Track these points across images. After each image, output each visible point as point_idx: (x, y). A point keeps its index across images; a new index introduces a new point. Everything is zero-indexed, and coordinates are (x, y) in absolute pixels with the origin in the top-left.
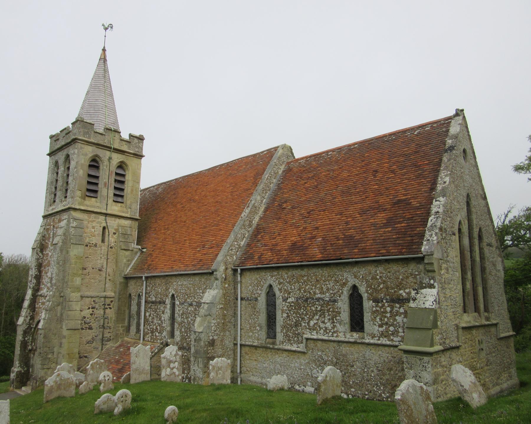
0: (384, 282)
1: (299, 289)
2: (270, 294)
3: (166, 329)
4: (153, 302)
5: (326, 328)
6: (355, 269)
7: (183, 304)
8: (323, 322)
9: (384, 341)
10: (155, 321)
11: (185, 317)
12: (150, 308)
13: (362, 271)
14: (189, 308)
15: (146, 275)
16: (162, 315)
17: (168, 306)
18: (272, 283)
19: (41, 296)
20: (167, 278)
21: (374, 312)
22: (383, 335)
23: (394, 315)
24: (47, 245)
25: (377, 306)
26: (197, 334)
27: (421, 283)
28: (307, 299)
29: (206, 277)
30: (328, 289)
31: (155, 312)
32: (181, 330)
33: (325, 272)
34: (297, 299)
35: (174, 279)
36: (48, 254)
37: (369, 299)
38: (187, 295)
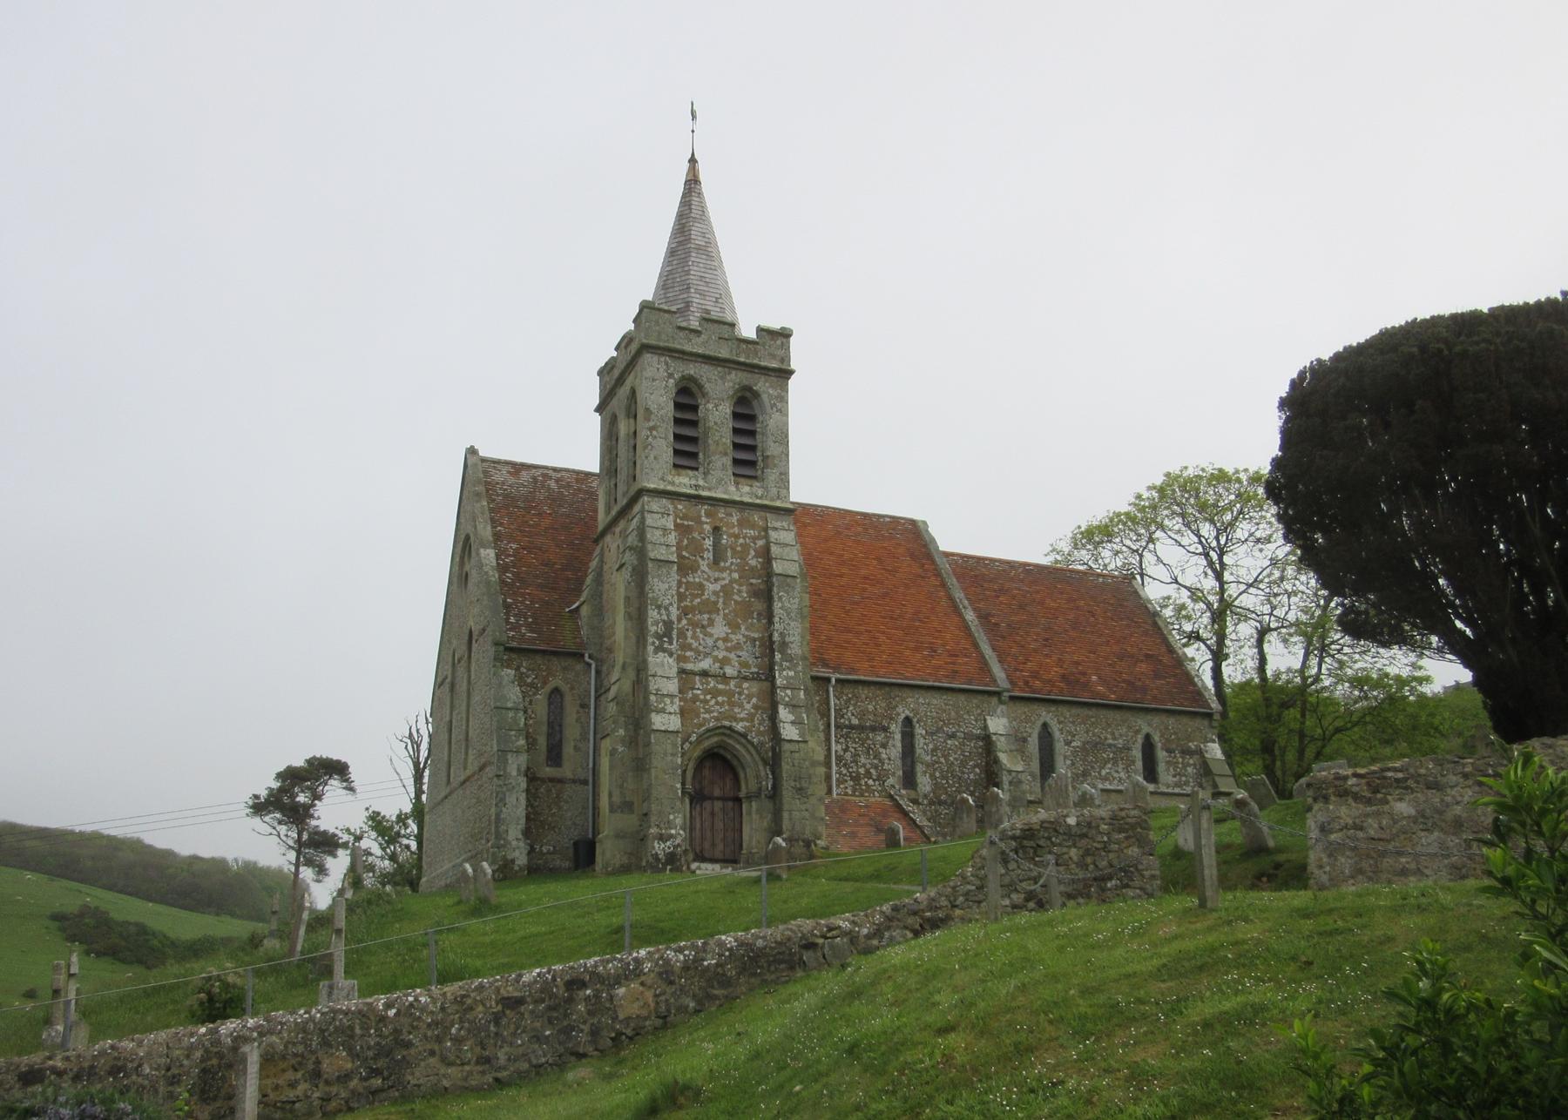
0: (1175, 733)
1: (1087, 732)
2: (1046, 735)
3: (894, 773)
4: (852, 727)
5: (1120, 778)
6: (1149, 717)
7: (932, 734)
8: (1117, 772)
9: (1177, 790)
10: (863, 760)
11: (940, 754)
12: (847, 736)
13: (1156, 720)
14: (949, 742)
15: (838, 676)
16: (881, 750)
17: (898, 736)
18: (1048, 720)
19: (705, 674)
20: (887, 689)
21: (1168, 763)
22: (1177, 785)
23: (1185, 766)
24: (687, 561)
25: (1170, 756)
26: (1014, 774)
27: (1206, 737)
28: (1097, 744)
29: (980, 697)
30: (1121, 735)
31: (863, 744)
32: (932, 777)
33: (1118, 715)
34: (1084, 743)
35: (906, 693)
36: (701, 586)
37: (1162, 749)
38: (943, 721)
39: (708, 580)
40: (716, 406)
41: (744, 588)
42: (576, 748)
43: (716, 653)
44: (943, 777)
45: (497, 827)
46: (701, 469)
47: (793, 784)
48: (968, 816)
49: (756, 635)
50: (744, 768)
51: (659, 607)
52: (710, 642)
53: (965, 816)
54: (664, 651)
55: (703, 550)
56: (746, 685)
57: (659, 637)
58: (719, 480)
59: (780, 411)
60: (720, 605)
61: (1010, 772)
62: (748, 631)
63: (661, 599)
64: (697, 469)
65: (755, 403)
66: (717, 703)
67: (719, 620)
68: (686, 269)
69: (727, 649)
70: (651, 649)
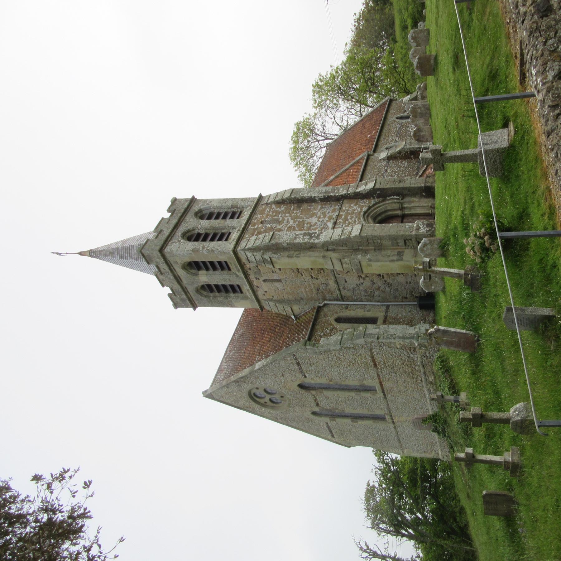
13: (390, 115)
39: (287, 225)
40: (200, 224)
41: (294, 212)
42: (369, 311)
43: (325, 221)
44: (405, 173)
45: (407, 338)
46: (231, 231)
47: (397, 184)
48: (422, 132)
49: (320, 207)
50: (386, 211)
51: (295, 238)
52: (319, 223)
53: (422, 134)
54: (319, 235)
55: (272, 227)
56: (344, 208)
57: (311, 237)
58: (238, 224)
59: (211, 202)
60: (301, 220)
61: (405, 145)
62: (317, 209)
63: (292, 238)
64: (230, 233)
65: (204, 212)
66: (351, 219)
67: (308, 220)
68: (131, 248)
69: (325, 216)
70: (317, 241)
